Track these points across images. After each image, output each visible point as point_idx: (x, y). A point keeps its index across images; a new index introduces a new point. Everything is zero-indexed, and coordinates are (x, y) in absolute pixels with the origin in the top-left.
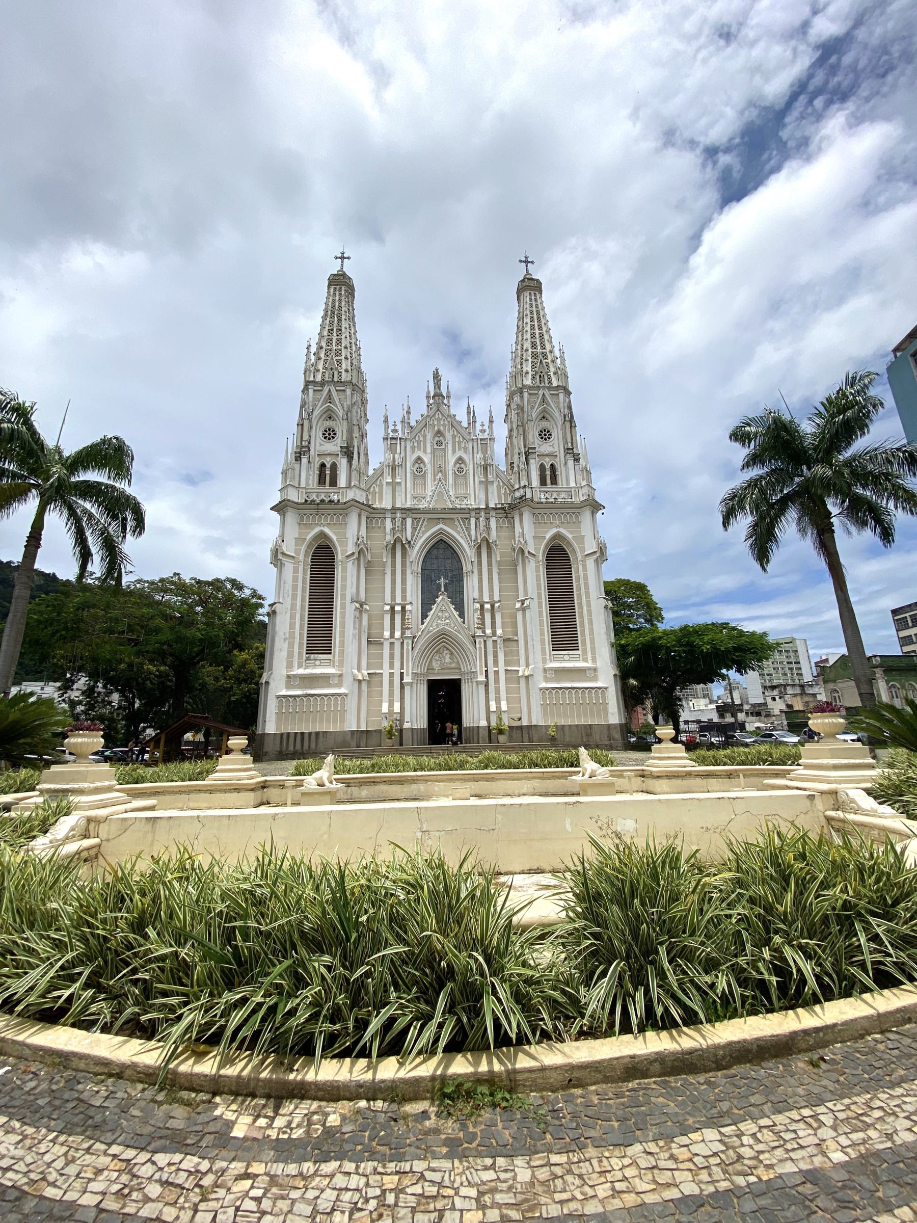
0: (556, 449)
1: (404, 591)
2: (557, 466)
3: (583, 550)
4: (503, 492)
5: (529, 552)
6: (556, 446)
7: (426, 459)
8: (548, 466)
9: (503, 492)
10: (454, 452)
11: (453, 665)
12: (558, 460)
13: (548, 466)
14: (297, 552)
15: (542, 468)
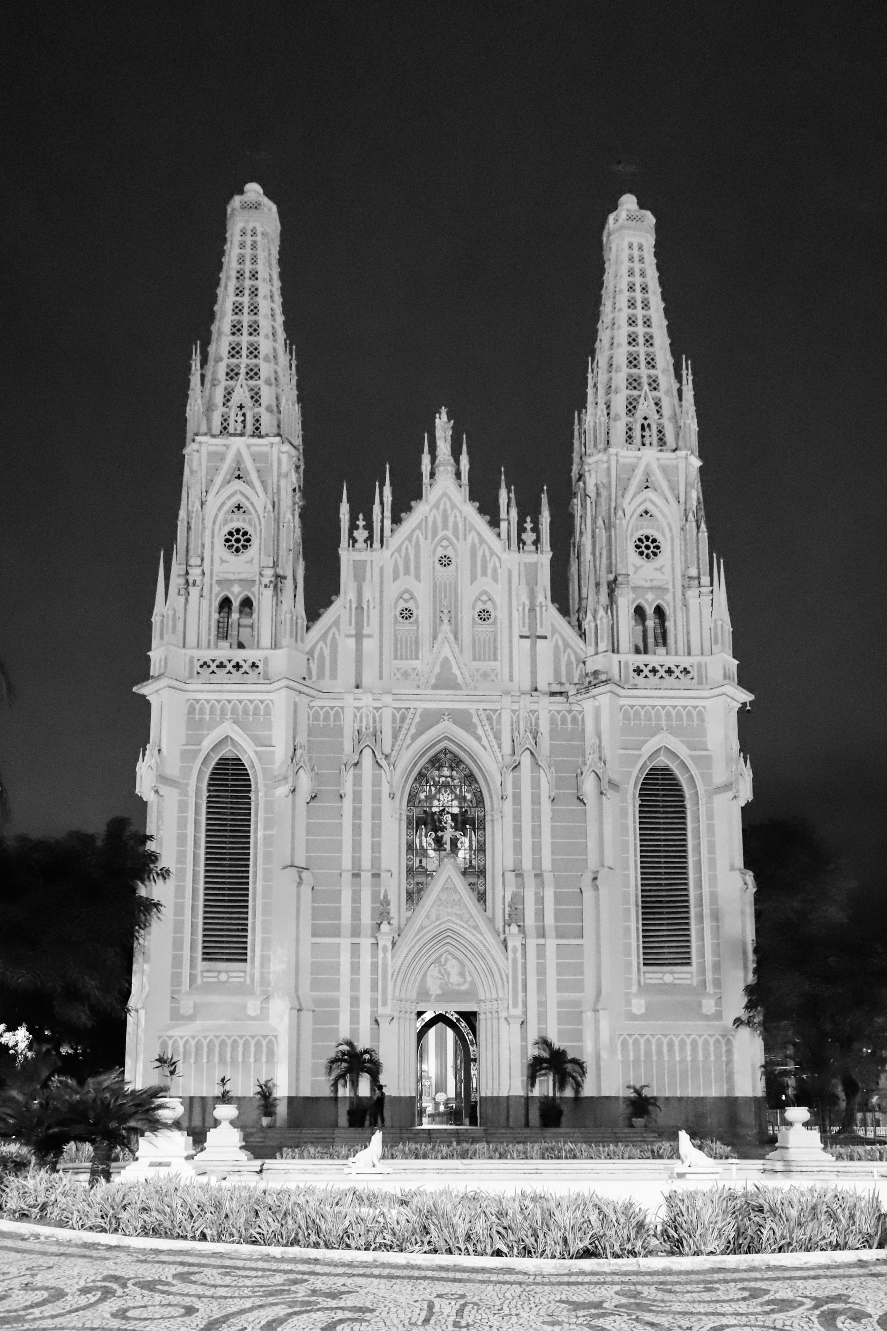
0: (668, 576)
1: (376, 848)
2: (668, 611)
3: (707, 778)
4: (564, 659)
5: (610, 782)
6: (667, 569)
7: (422, 592)
8: (650, 611)
9: (564, 659)
10: (473, 579)
11: (465, 987)
12: (669, 597)
13: (650, 611)
14: (186, 772)
15: (639, 612)
